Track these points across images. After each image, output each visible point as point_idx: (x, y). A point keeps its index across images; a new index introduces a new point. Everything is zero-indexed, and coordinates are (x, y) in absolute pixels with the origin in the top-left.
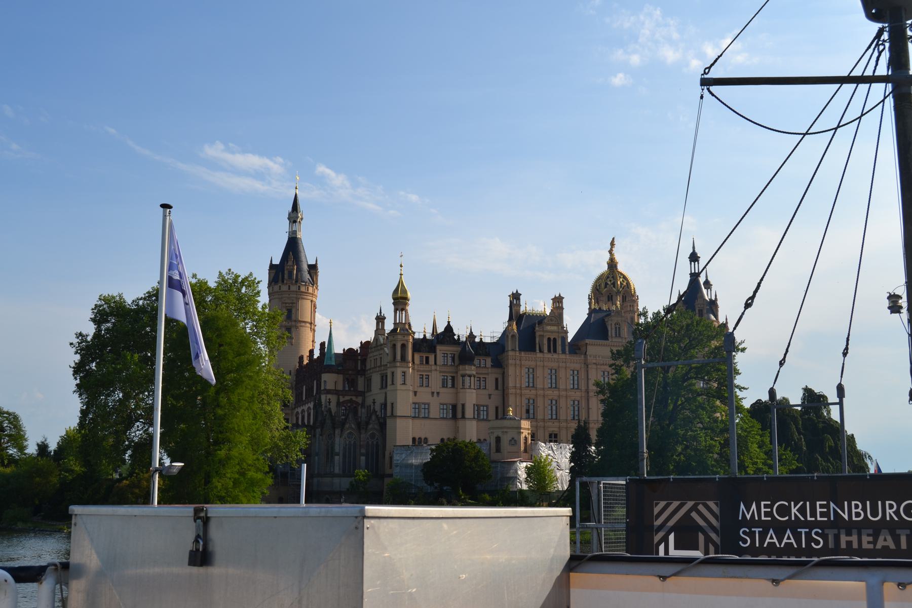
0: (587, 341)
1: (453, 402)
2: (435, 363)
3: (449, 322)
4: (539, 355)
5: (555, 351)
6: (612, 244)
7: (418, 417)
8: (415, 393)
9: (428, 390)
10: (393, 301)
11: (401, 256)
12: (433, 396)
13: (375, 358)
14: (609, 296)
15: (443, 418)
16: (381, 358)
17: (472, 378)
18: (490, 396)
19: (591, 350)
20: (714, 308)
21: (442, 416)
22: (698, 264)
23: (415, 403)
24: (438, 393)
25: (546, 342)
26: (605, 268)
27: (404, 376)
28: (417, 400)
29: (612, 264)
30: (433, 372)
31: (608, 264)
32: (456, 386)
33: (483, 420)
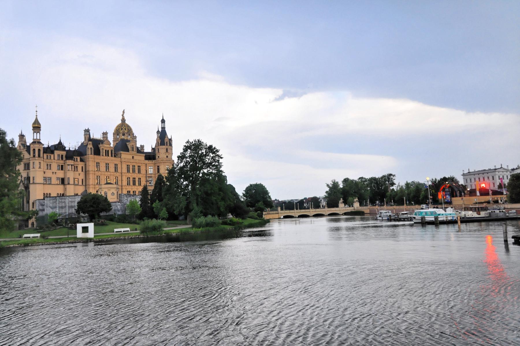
0: (121, 152)
3: (60, 140)
5: (108, 156)
7: (46, 184)
8: (44, 172)
9: (51, 171)
10: (32, 128)
15: (57, 184)
17: (73, 166)
21: (57, 183)
23: (44, 177)
24: (55, 173)
27: (40, 164)
28: (45, 175)
33: (76, 185)
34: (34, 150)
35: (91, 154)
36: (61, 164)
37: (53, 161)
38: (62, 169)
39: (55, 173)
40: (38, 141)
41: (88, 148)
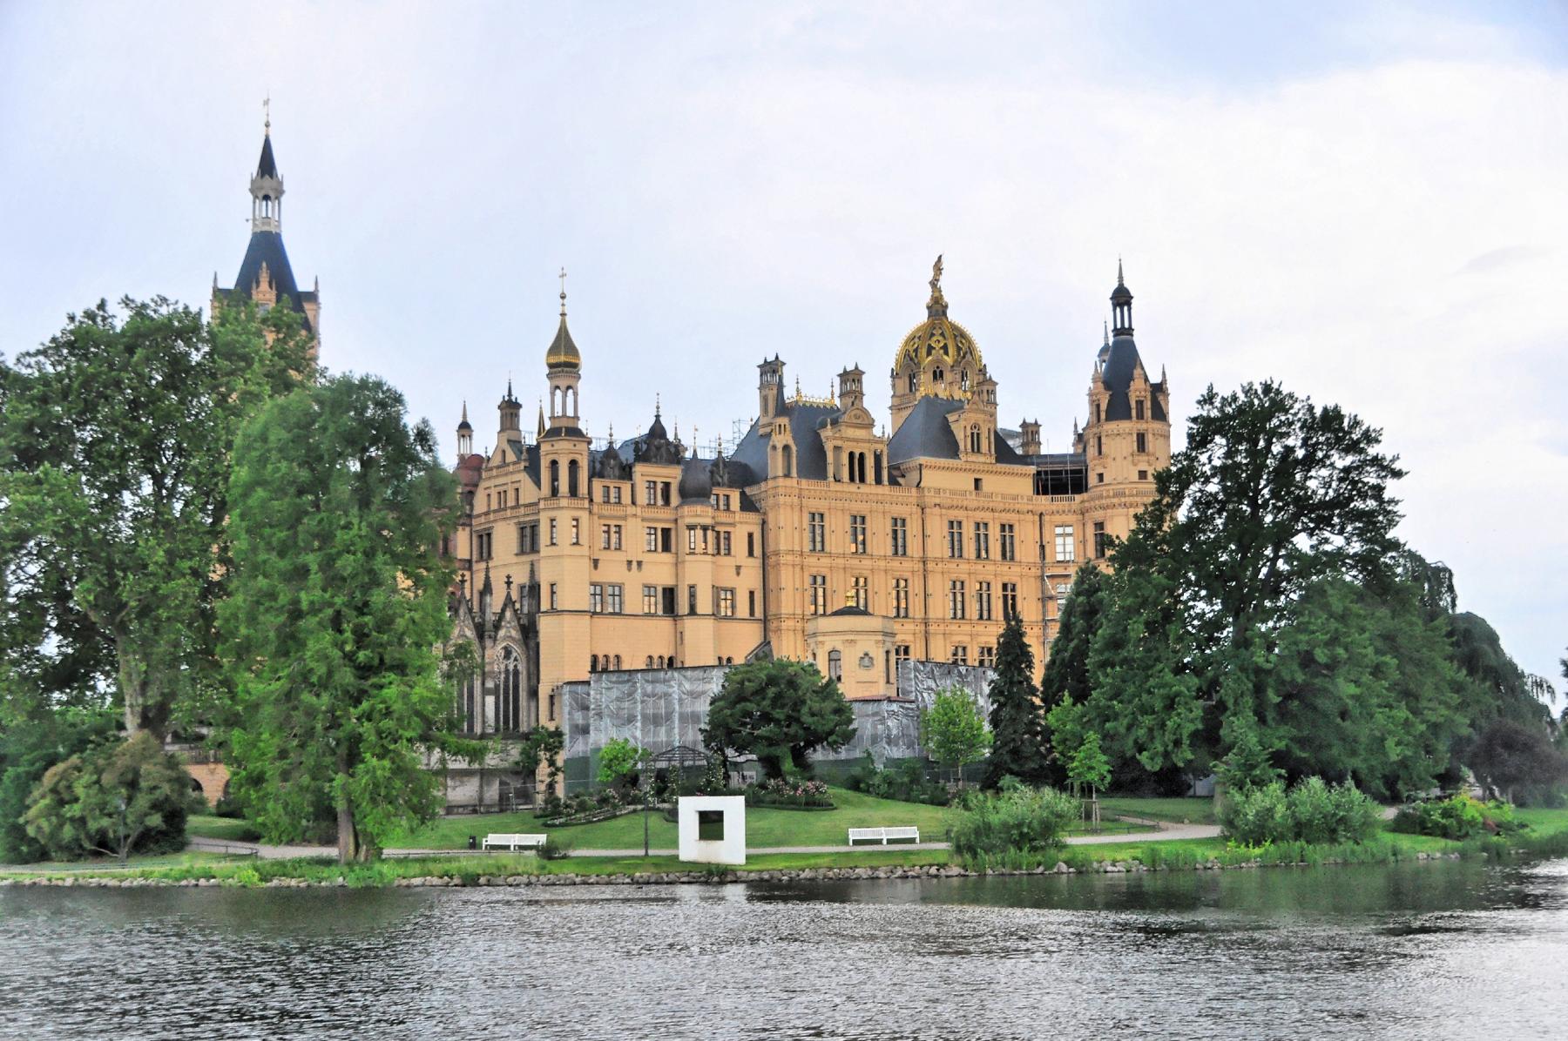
0: (923, 460)
1: (670, 582)
2: (634, 503)
3: (658, 417)
4: (835, 487)
5: (862, 480)
6: (938, 268)
7: (601, 613)
8: (596, 563)
9: (621, 557)
10: (547, 370)
11: (563, 276)
12: (629, 570)
13: (501, 489)
14: (935, 372)
15: (649, 615)
16: (517, 490)
17: (709, 533)
18: (738, 568)
19: (931, 479)
20: (1161, 398)
21: (646, 610)
22: (1129, 310)
23: (594, 584)
24: (639, 563)
25: (845, 460)
26: (922, 317)
27: (576, 527)
28: (599, 577)
29: (937, 308)
30: (629, 519)
31: (928, 308)
32: (673, 549)
33: (726, 617)
34: (554, 463)
35: (787, 475)
36: (660, 526)
37: (631, 510)
38: (666, 547)
39: (639, 563)
40: (570, 424)
41: (774, 448)
